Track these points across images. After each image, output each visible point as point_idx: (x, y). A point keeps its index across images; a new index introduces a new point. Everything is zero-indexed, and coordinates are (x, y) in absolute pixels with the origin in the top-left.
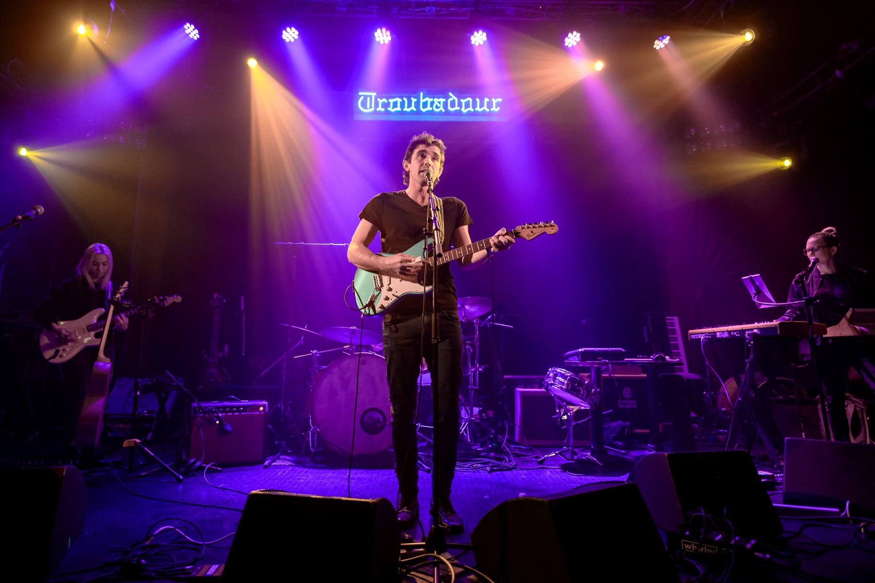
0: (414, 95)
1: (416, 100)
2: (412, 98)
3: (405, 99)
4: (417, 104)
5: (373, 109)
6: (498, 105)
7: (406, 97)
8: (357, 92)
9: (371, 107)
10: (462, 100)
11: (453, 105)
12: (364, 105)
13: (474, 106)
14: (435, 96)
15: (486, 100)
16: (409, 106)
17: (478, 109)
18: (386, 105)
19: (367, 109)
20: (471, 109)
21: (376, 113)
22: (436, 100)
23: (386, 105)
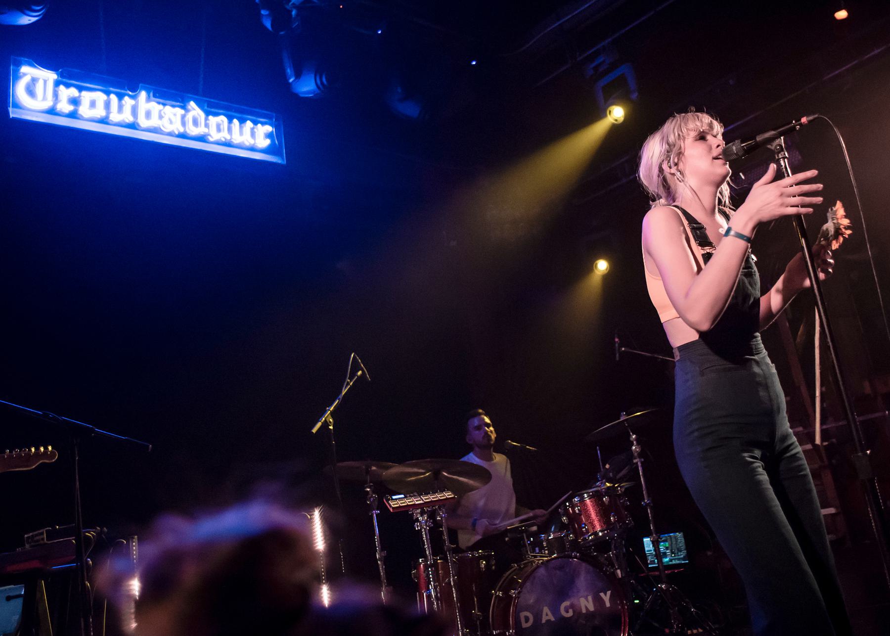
0: (130, 93)
1: (133, 102)
2: (126, 98)
3: (113, 97)
4: (134, 111)
5: (48, 104)
6: (269, 136)
7: (118, 95)
8: (18, 65)
9: (45, 98)
10: (211, 117)
11: (195, 122)
12: (30, 91)
13: (230, 130)
14: (168, 102)
15: (249, 124)
16: (120, 108)
17: (237, 138)
18: (75, 102)
19: (36, 100)
20: (224, 135)
21: (52, 111)
22: (168, 108)
23: (75, 102)
